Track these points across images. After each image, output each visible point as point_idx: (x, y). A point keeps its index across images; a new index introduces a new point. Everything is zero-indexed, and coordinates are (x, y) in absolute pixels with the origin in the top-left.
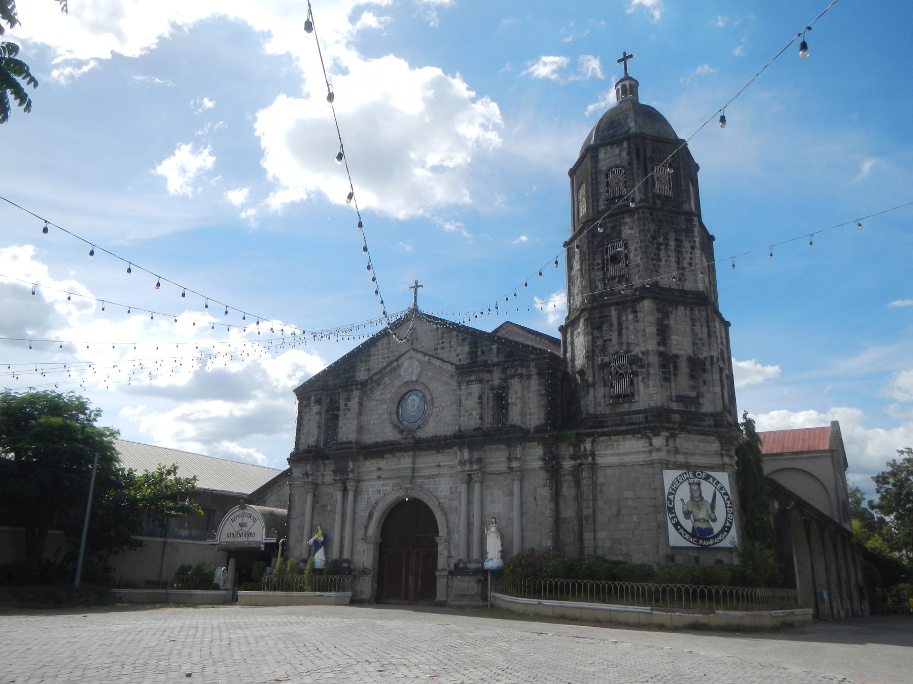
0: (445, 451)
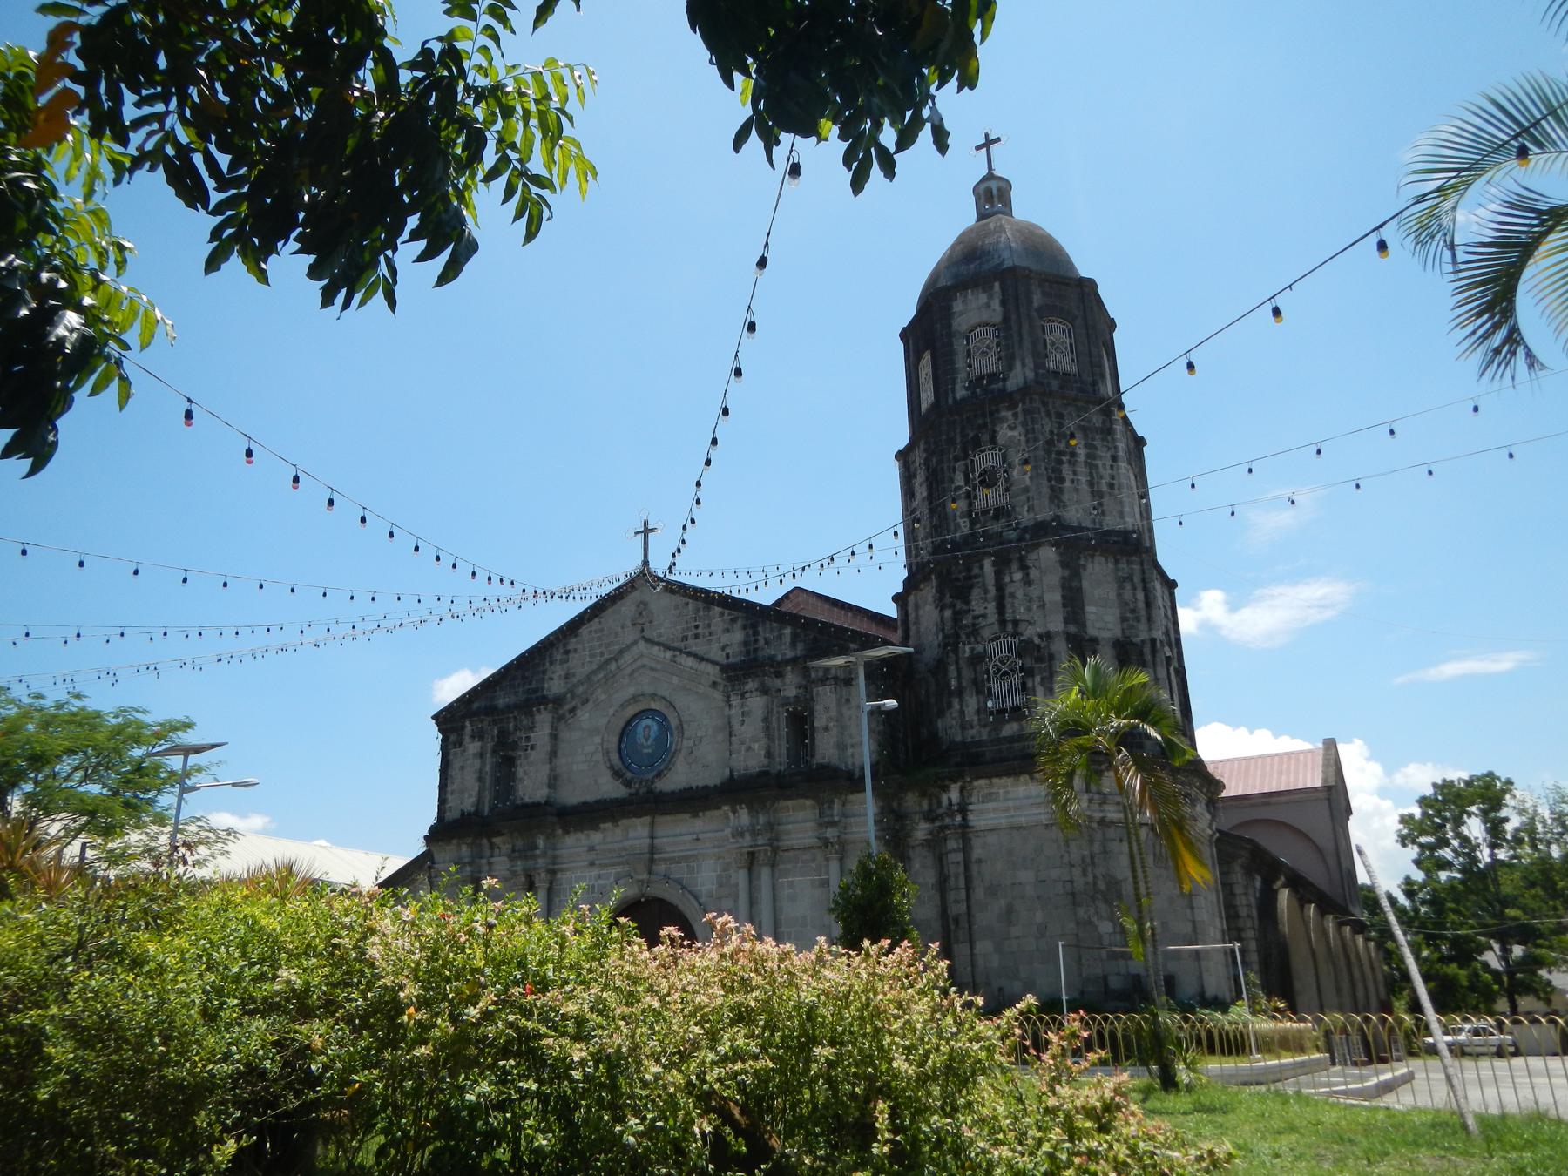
0: (708, 813)
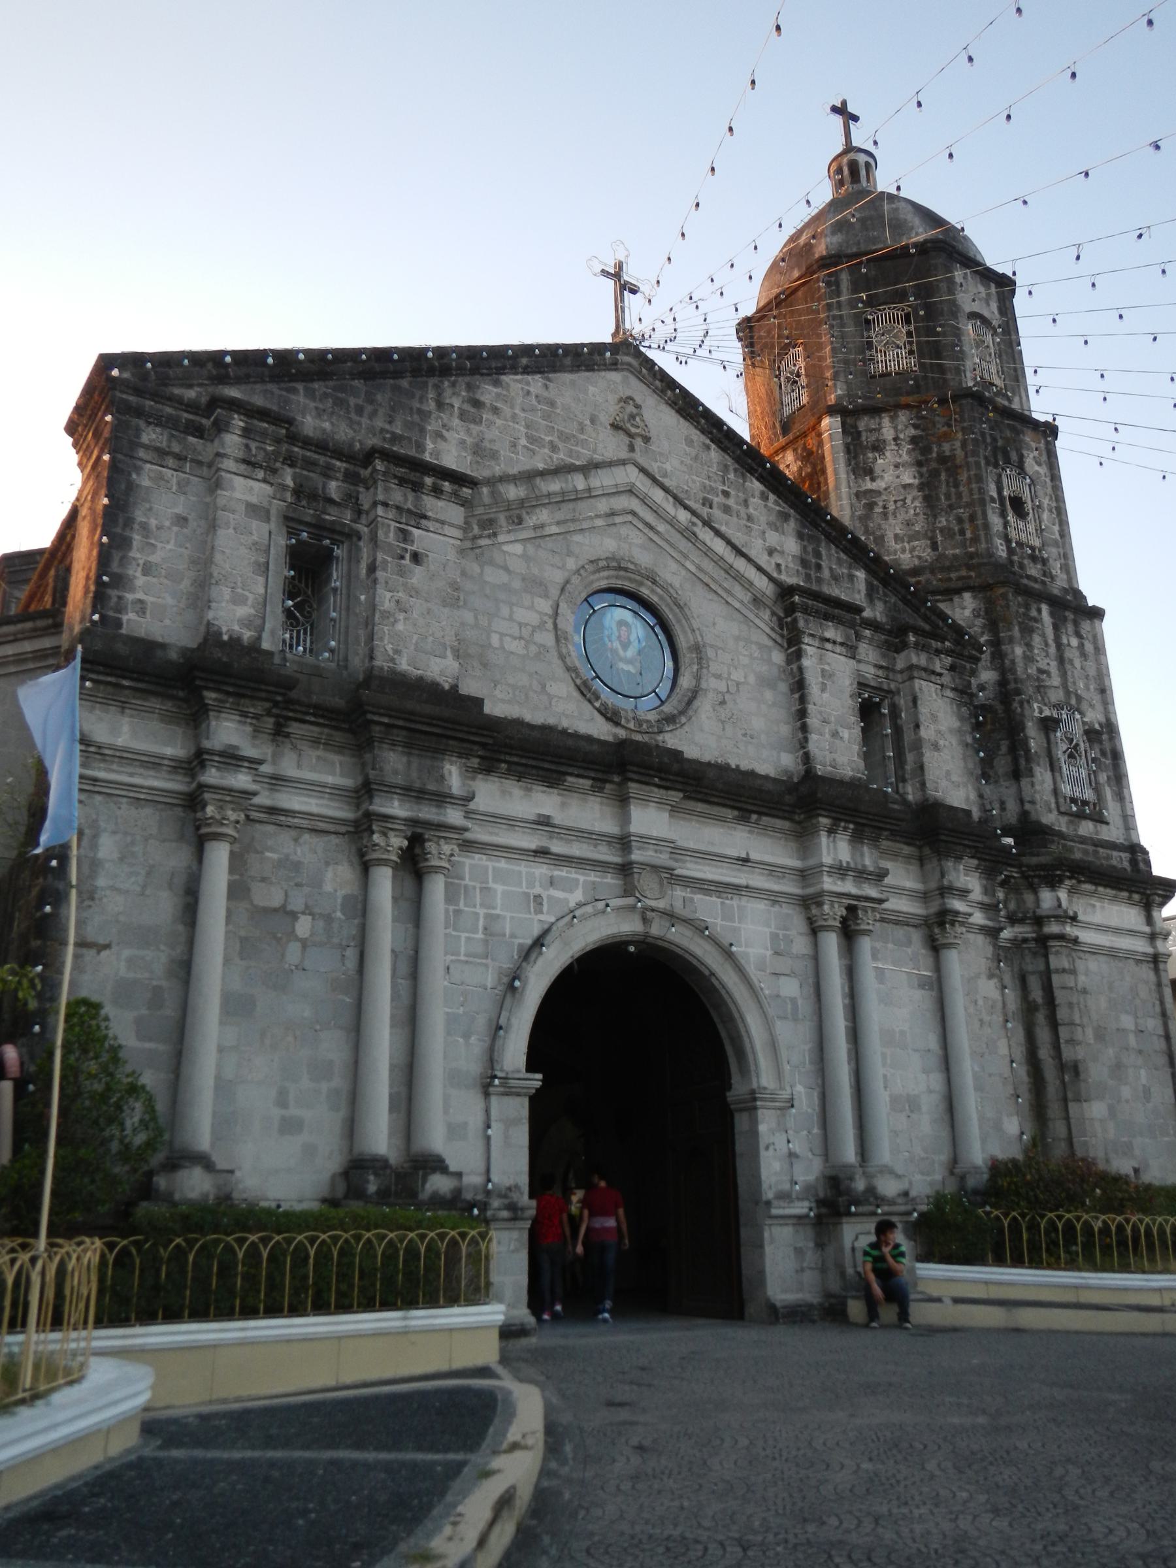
0: (765, 820)
